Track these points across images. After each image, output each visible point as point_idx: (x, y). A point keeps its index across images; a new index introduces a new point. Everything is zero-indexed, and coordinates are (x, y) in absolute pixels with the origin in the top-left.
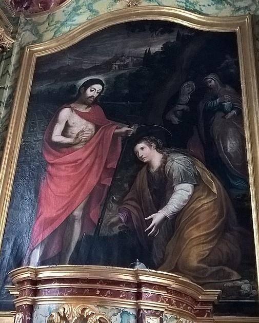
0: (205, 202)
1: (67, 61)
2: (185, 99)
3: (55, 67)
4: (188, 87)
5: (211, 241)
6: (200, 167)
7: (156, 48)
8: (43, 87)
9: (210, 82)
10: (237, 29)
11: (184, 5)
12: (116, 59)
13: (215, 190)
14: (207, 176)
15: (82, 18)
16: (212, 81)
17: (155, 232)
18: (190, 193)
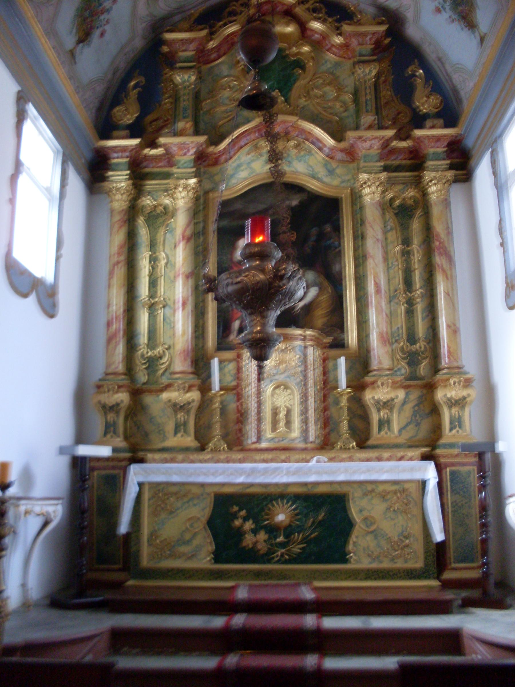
0: (325, 298)
1: (238, 206)
2: (313, 238)
3: (232, 209)
4: (314, 231)
5: (329, 315)
6: (321, 279)
7: (295, 203)
8: (225, 223)
9: (328, 228)
10: (343, 196)
11: (311, 173)
12: (271, 207)
13: (330, 291)
14: (326, 283)
15: (243, 174)
16: (328, 228)
17: (300, 312)
18: (317, 292)
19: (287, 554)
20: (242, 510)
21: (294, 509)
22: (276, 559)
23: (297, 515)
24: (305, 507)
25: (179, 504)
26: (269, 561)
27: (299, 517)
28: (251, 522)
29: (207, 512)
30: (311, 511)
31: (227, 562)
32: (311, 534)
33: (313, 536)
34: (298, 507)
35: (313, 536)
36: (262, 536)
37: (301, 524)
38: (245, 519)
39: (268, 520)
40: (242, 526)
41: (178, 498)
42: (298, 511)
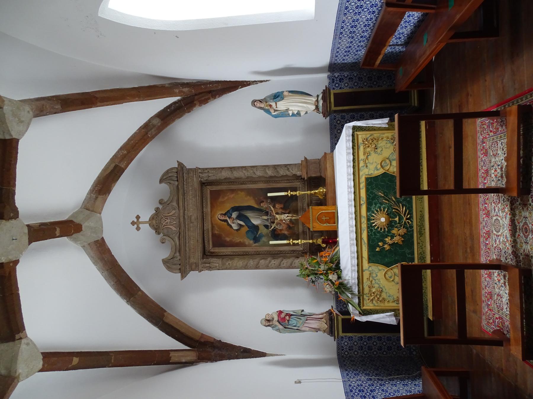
19: (407, 216)
20: (379, 245)
21: (377, 211)
22: (410, 223)
23: (381, 210)
24: (376, 204)
25: (376, 286)
26: (412, 227)
27: (382, 209)
28: (387, 239)
29: (381, 267)
30: (378, 201)
31: (413, 253)
32: (393, 201)
33: (394, 199)
34: (375, 209)
35: (394, 199)
36: (395, 231)
37: (387, 208)
38: (385, 243)
39: (384, 229)
40: (390, 245)
41: (373, 286)
42: (378, 210)
